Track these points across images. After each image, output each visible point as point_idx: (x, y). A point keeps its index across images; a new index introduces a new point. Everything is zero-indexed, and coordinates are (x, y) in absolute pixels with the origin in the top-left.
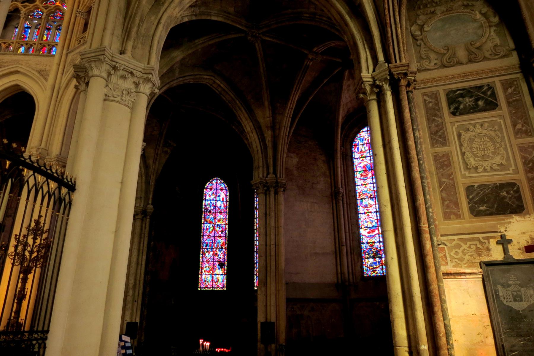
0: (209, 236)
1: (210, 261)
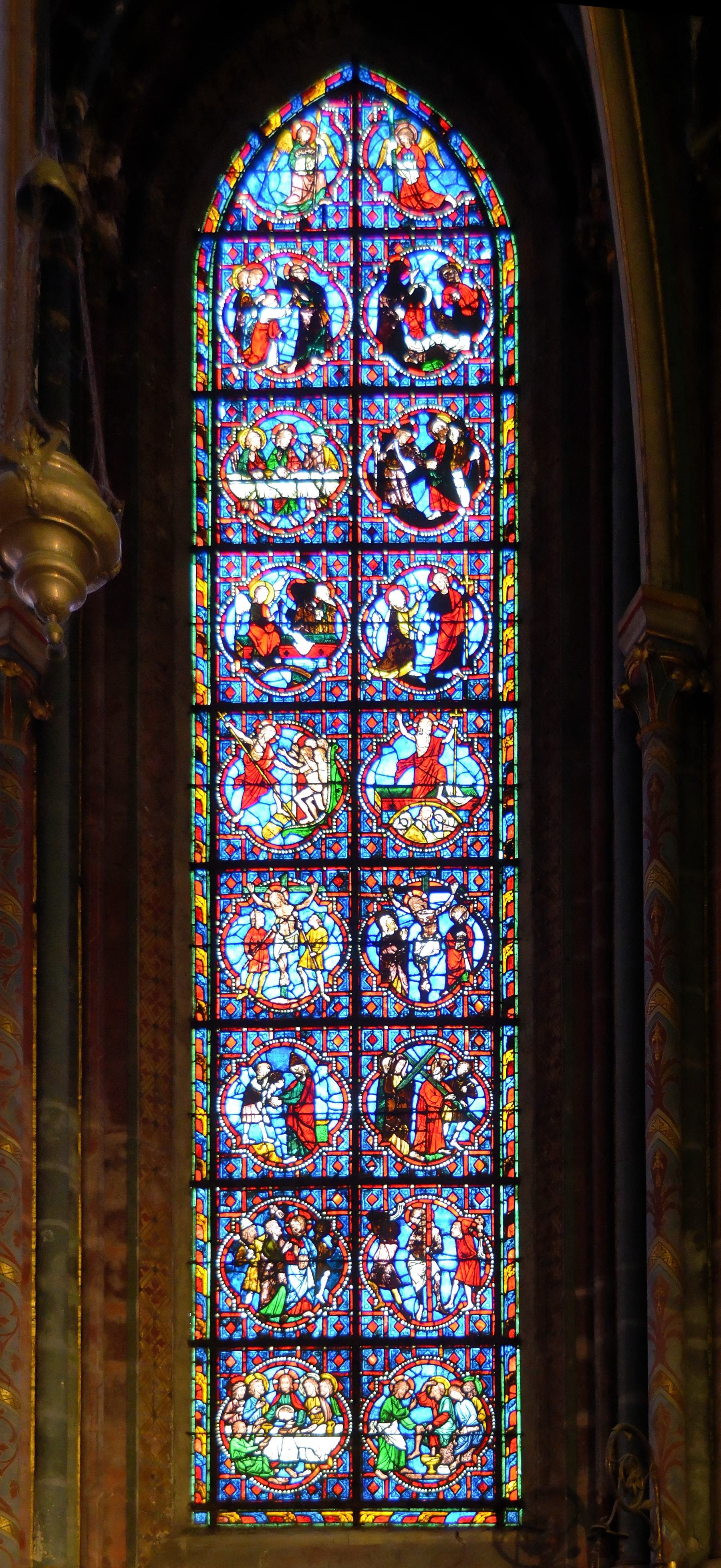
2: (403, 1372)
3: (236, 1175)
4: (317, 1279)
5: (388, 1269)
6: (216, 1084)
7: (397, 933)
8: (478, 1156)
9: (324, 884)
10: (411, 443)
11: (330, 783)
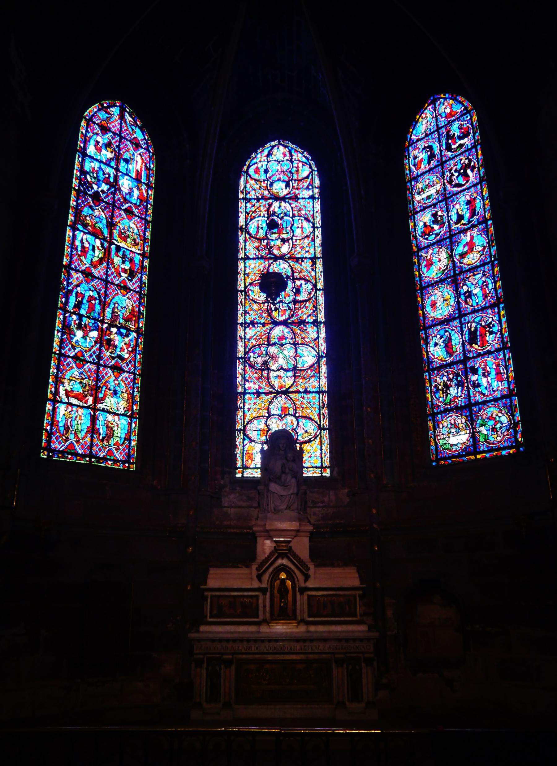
0: (87, 274)
1: (88, 362)
2: (484, 412)
3: (434, 366)
4: (458, 390)
5: (476, 382)
6: (427, 344)
7: (468, 290)
8: (497, 343)
9: (448, 284)
10: (456, 169)
11: (447, 258)
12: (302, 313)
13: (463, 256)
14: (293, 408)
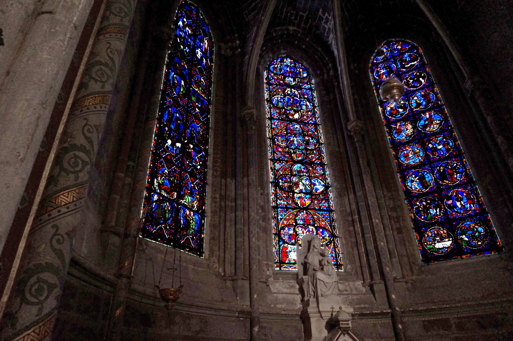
2: (462, 224)
4: (436, 210)
12: (312, 157)
13: (425, 126)
14: (312, 220)
